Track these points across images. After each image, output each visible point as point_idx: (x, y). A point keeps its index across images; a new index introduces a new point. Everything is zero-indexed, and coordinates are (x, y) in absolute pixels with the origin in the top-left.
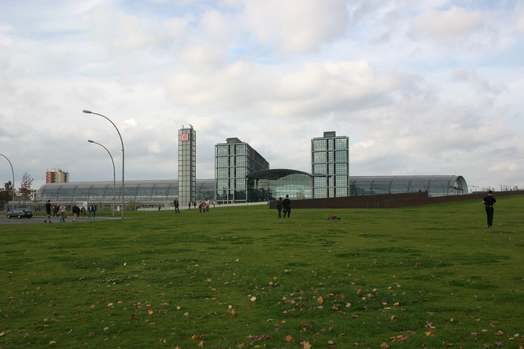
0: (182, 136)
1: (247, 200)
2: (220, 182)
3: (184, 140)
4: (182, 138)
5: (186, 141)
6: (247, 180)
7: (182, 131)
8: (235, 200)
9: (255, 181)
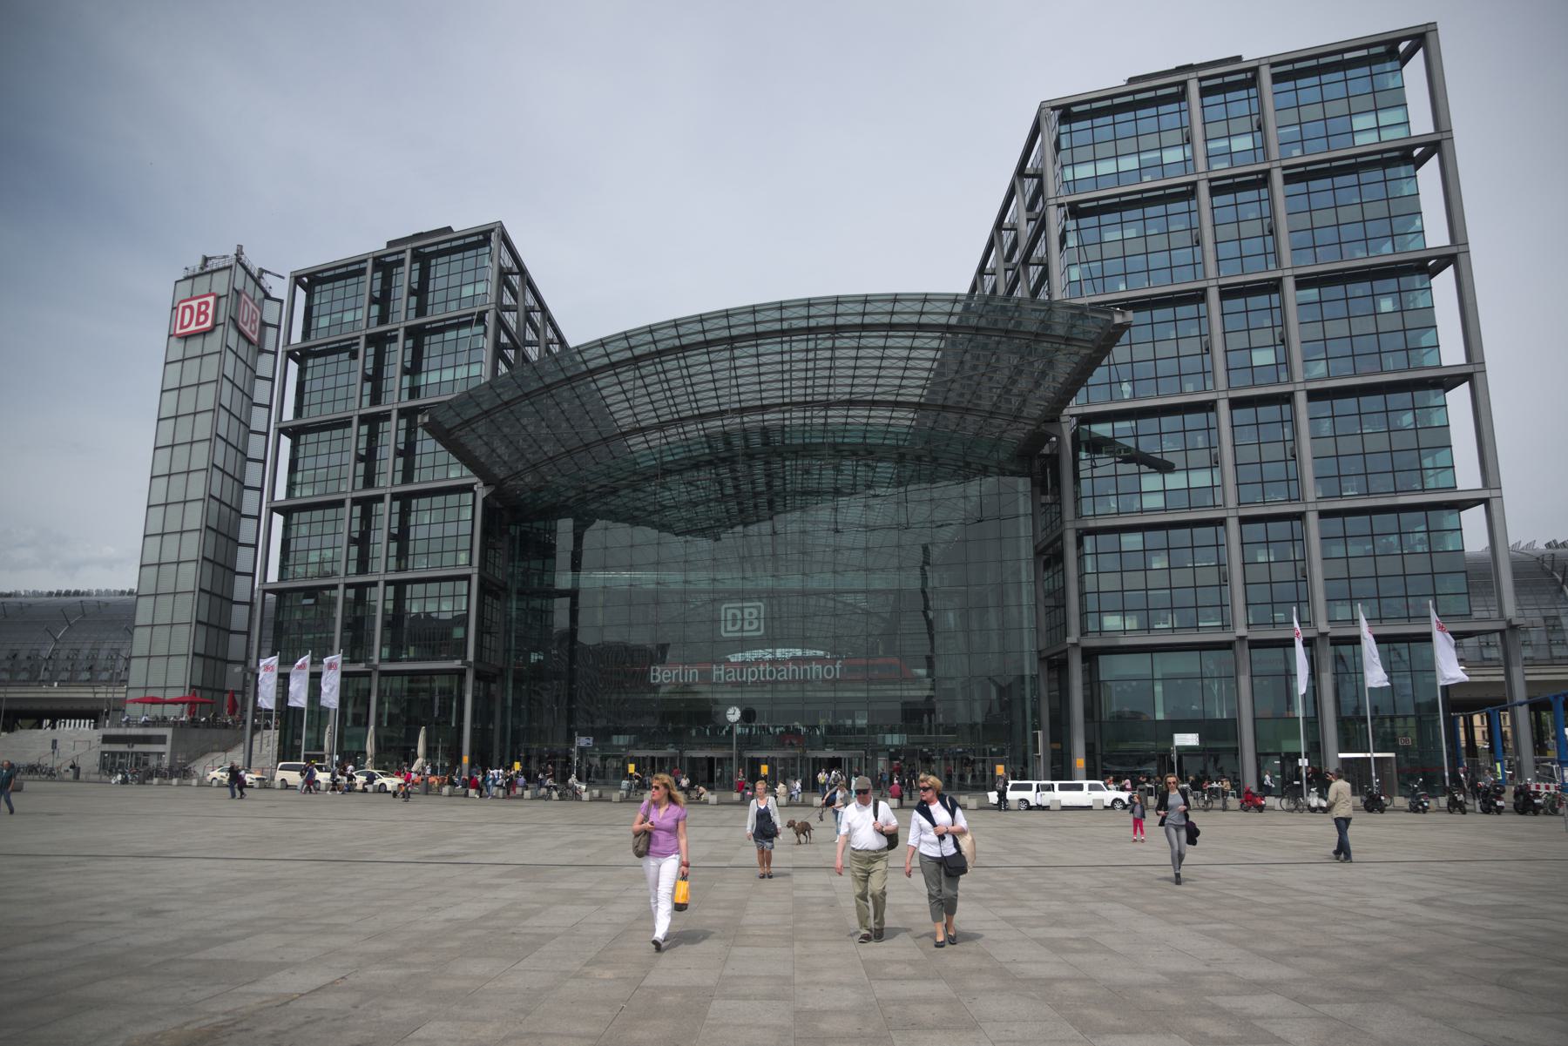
0: (184, 308)
1: (471, 658)
2: (304, 530)
3: (193, 328)
4: (186, 322)
5: (204, 333)
6: (485, 500)
7: (190, 281)
8: (381, 660)
9: (565, 526)
